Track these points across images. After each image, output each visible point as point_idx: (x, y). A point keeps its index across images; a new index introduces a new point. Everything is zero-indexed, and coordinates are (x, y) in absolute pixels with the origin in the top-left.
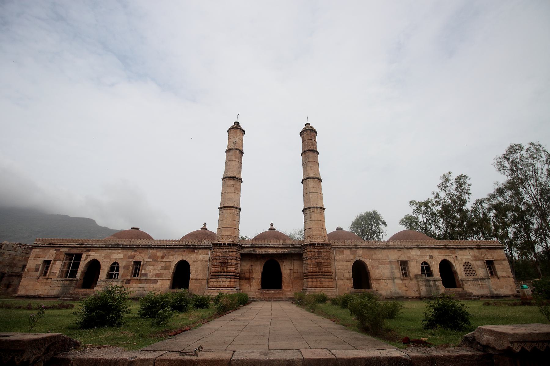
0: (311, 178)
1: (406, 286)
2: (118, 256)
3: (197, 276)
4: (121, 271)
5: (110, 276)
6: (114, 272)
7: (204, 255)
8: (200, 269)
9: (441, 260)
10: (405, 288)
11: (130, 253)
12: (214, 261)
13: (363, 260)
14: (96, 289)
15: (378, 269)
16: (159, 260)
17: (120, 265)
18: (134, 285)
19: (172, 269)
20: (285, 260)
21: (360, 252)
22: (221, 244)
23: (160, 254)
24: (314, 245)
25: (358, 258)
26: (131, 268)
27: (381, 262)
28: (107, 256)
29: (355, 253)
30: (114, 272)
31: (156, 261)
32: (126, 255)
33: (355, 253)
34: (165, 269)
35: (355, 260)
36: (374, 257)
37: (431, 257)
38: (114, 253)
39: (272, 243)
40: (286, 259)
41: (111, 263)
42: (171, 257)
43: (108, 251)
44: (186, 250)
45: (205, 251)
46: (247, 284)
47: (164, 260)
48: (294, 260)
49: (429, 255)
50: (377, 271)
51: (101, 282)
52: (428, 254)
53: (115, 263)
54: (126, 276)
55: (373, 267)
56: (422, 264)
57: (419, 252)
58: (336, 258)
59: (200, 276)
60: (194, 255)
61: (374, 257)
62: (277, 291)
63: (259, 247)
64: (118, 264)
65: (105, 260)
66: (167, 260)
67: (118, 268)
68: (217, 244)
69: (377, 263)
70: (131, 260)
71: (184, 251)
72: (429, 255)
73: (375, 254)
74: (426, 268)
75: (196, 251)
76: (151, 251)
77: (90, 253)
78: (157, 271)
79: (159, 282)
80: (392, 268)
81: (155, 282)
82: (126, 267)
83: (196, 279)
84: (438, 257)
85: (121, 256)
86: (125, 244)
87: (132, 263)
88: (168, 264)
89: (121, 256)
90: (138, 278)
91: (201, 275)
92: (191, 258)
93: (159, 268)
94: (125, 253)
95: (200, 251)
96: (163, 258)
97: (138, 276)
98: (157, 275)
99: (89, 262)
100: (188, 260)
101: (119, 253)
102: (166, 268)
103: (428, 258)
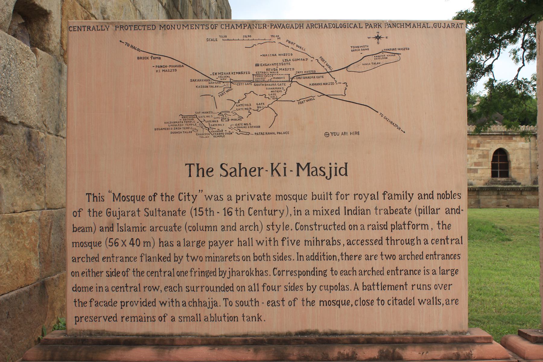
3: (519, 164)
8: (521, 157)
16: (474, 148)
19: (491, 158)
31: (472, 149)
34: (483, 158)
42: (488, 145)
44: (503, 137)
47: (480, 148)
59: (522, 165)
60: (513, 143)
66: (484, 149)
71: (501, 139)
75: (514, 138)
78: (475, 160)
79: (479, 171)
81: (475, 171)
83: (519, 168)
88: (485, 153)
91: (524, 164)
92: (509, 146)
93: (477, 156)
96: (478, 146)
98: (476, 164)
100: (506, 148)
102: (484, 156)
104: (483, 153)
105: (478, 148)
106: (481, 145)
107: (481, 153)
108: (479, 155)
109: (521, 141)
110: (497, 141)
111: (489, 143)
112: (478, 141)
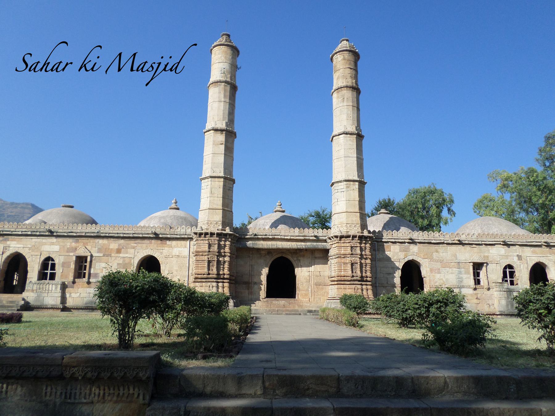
0: (347, 134)
1: (477, 298)
2: (51, 247)
4: (58, 270)
5: (42, 276)
6: (49, 271)
7: (181, 249)
8: (175, 268)
9: (534, 263)
10: (476, 301)
11: (69, 243)
12: (199, 258)
13: (418, 259)
14: (25, 295)
15: (439, 273)
16: (113, 255)
17: (56, 262)
18: (80, 290)
20: (301, 259)
21: (414, 248)
22: (206, 234)
23: (114, 245)
24: (348, 237)
25: (410, 258)
26: (73, 266)
27: (445, 264)
28: (33, 248)
29: (406, 250)
30: (49, 271)
31: (110, 255)
32: (64, 247)
33: (406, 250)
35: (406, 260)
36: (435, 255)
37: (520, 257)
38: (45, 244)
39: (282, 234)
40: (303, 256)
41: (43, 258)
43: (35, 240)
44: (153, 241)
45: (183, 242)
46: (247, 291)
47: (121, 255)
48: (316, 258)
49: (518, 256)
50: (438, 276)
51: (31, 285)
52: (516, 254)
53: (49, 259)
54: (66, 277)
55: (431, 270)
56: (505, 268)
57: (502, 250)
58: (378, 257)
60: (166, 248)
61: (435, 255)
62: (291, 300)
63: (264, 239)
64: (53, 260)
65: (33, 253)
66: (126, 255)
67: (53, 267)
68: (201, 234)
69: (438, 265)
70: (72, 254)
71: (151, 243)
72: (518, 256)
73: (437, 252)
74: (509, 272)
76: (101, 241)
77: (8, 243)
80: (460, 273)
82: (64, 264)
84: (532, 257)
85: (56, 248)
86: (61, 231)
87: (74, 258)
88: (127, 261)
89: (56, 248)
90: (86, 280)
94: (61, 244)
95: (174, 243)
96: (119, 251)
97: (84, 277)
99: (8, 257)
101: (52, 244)
103: (516, 259)
104: (124, 261)
105: (117, 255)
106: (123, 250)
107: (121, 262)
108: (118, 264)
109: (178, 247)
110: (144, 245)
111: (133, 248)
112: (119, 245)
